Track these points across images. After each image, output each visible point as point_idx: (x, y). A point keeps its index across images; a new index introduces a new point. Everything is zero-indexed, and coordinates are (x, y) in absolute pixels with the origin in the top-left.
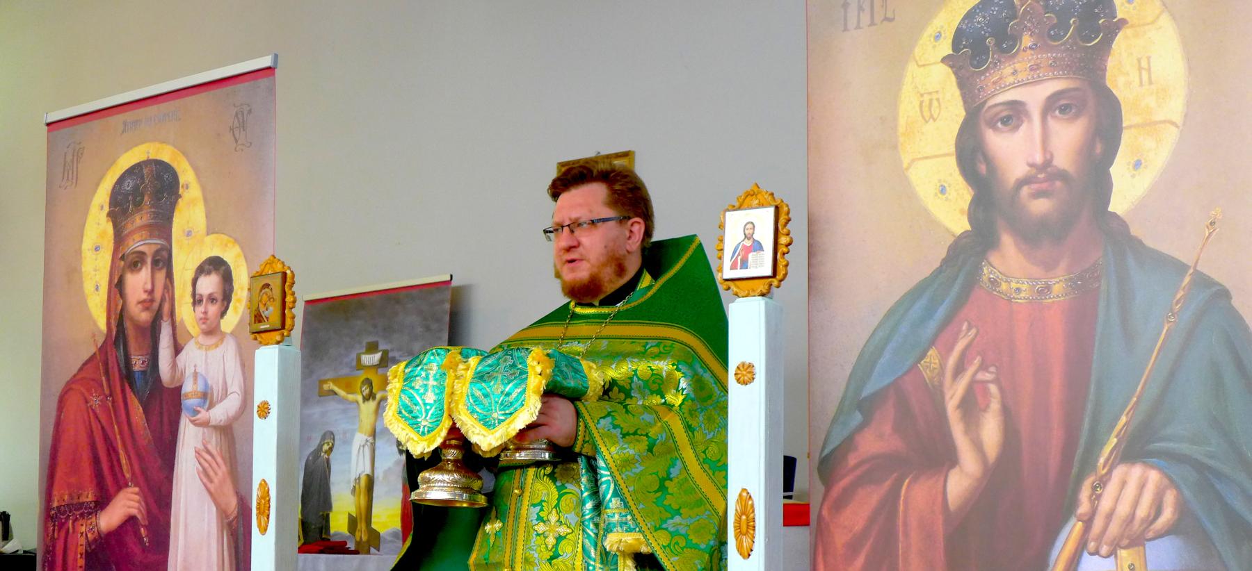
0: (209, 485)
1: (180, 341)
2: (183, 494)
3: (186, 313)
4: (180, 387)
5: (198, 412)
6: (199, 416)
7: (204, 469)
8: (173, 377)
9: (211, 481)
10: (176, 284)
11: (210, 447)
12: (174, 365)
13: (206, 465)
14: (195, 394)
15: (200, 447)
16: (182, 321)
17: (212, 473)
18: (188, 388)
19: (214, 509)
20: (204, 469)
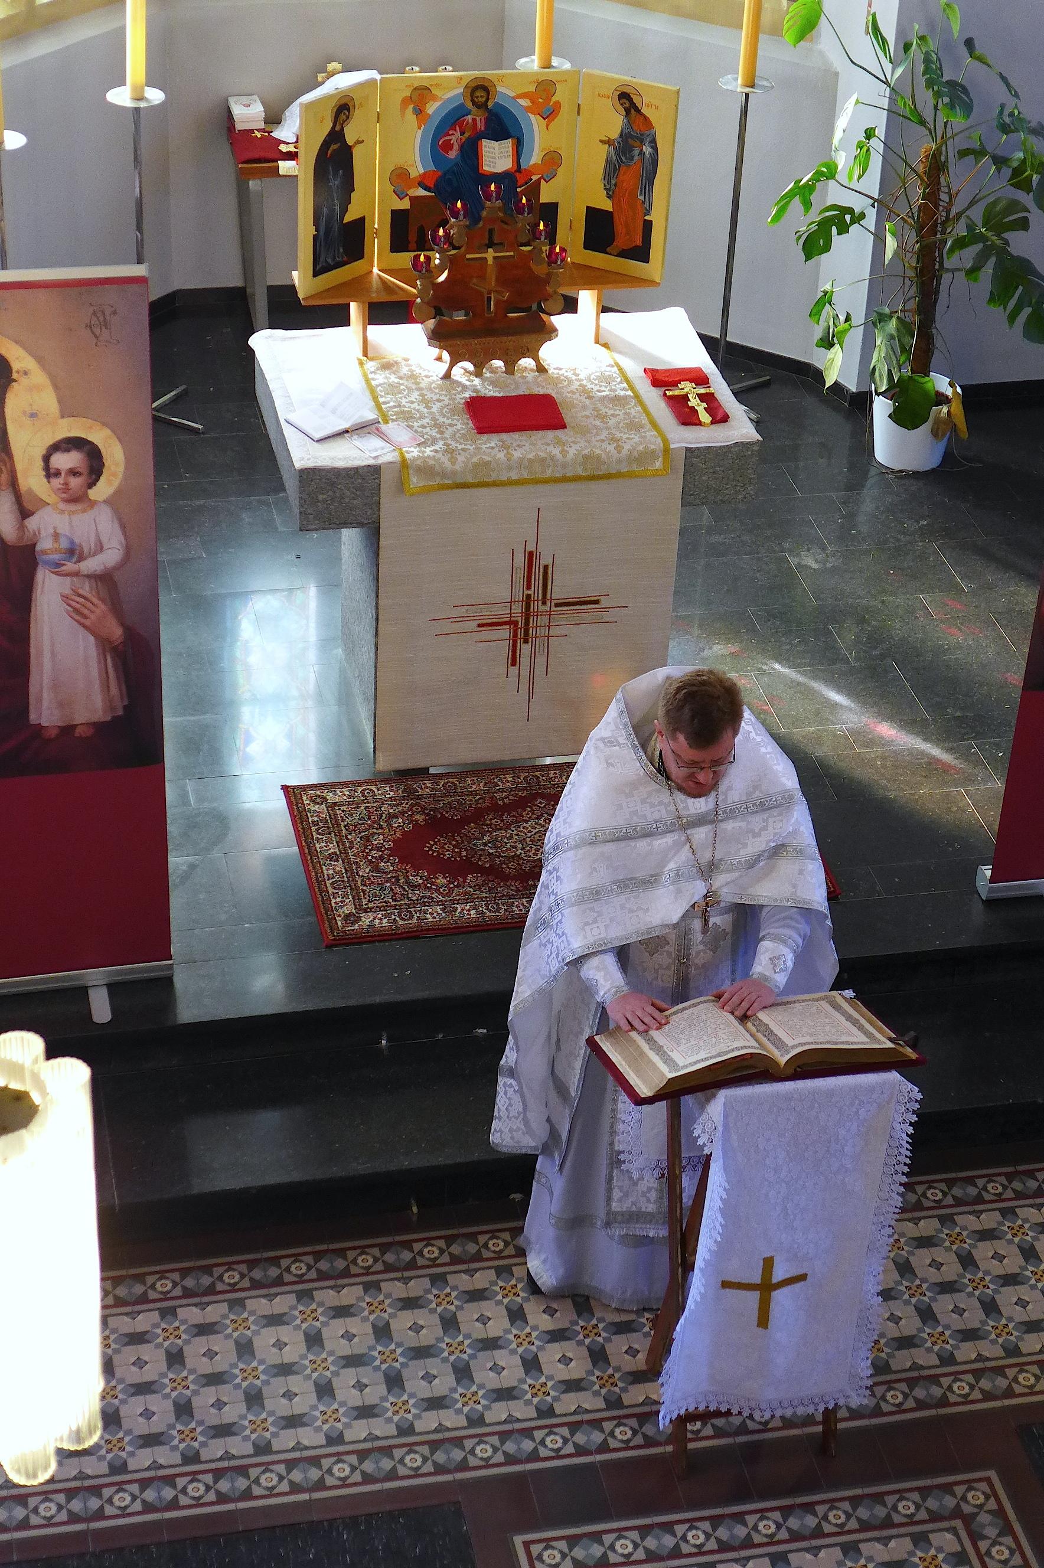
0: (87, 622)
1: (28, 505)
2: (46, 630)
3: (33, 480)
4: (34, 545)
5: (63, 565)
6: (63, 568)
7: (76, 610)
8: (21, 538)
9: (86, 618)
10: (15, 458)
11: (81, 592)
12: (22, 528)
13: (78, 606)
14: (57, 551)
15: (68, 591)
16: (30, 491)
17: (86, 612)
18: (45, 544)
19: (92, 638)
20: (76, 610)
